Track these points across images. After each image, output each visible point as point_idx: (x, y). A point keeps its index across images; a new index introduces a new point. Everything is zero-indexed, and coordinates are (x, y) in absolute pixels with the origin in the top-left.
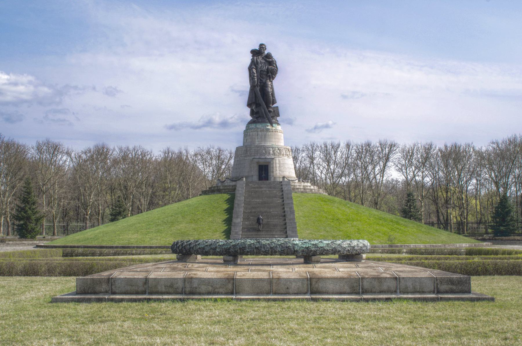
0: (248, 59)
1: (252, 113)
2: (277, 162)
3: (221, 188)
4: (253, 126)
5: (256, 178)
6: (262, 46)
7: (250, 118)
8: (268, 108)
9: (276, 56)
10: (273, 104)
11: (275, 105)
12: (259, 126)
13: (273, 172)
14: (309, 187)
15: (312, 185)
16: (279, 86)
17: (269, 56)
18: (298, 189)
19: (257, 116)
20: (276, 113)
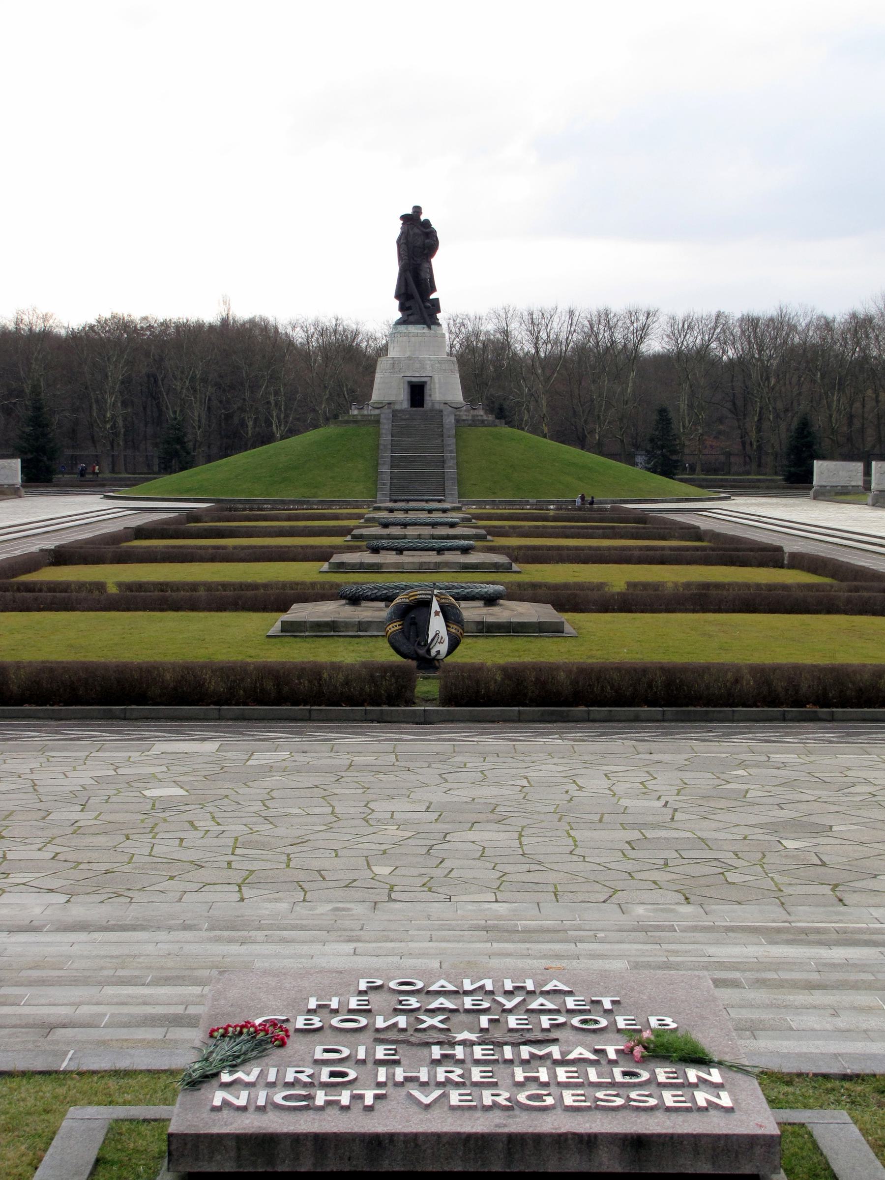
0: (396, 228)
1: (402, 308)
2: (436, 381)
3: (359, 418)
4: (402, 328)
5: (406, 405)
6: (417, 210)
7: (399, 315)
8: (423, 302)
9: (434, 225)
10: (432, 293)
11: (432, 297)
12: (412, 329)
13: (430, 396)
14: (480, 418)
15: (486, 413)
16: (439, 264)
17: (427, 223)
18: (464, 420)
19: (409, 312)
20: (435, 306)
